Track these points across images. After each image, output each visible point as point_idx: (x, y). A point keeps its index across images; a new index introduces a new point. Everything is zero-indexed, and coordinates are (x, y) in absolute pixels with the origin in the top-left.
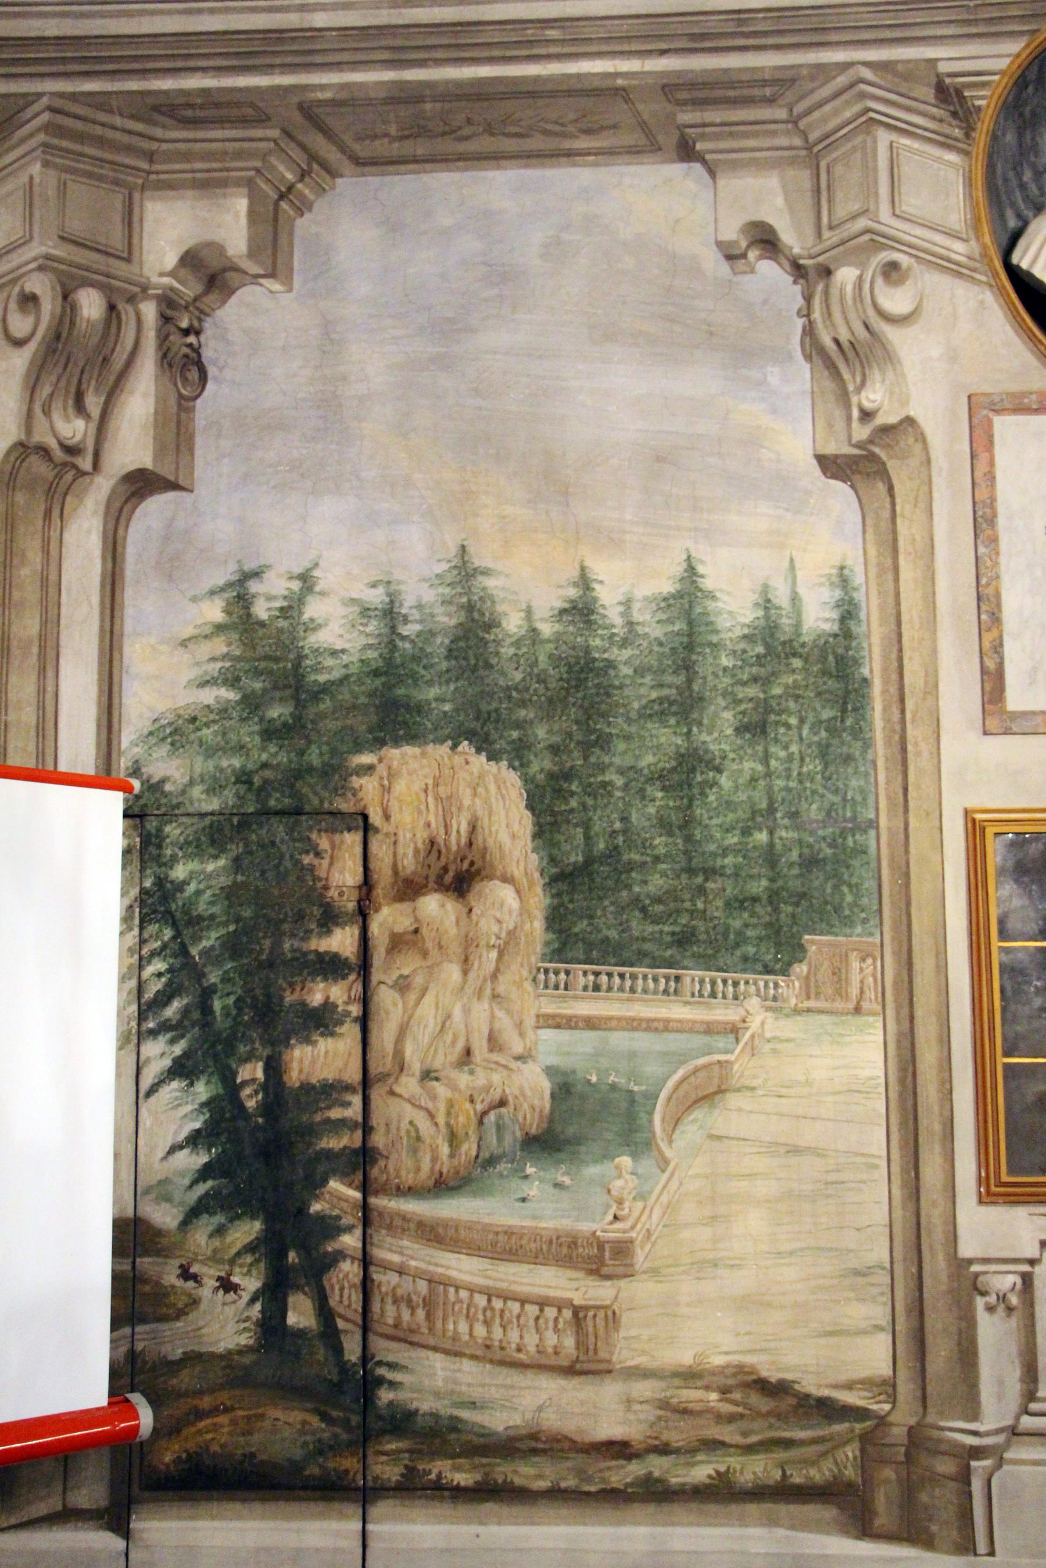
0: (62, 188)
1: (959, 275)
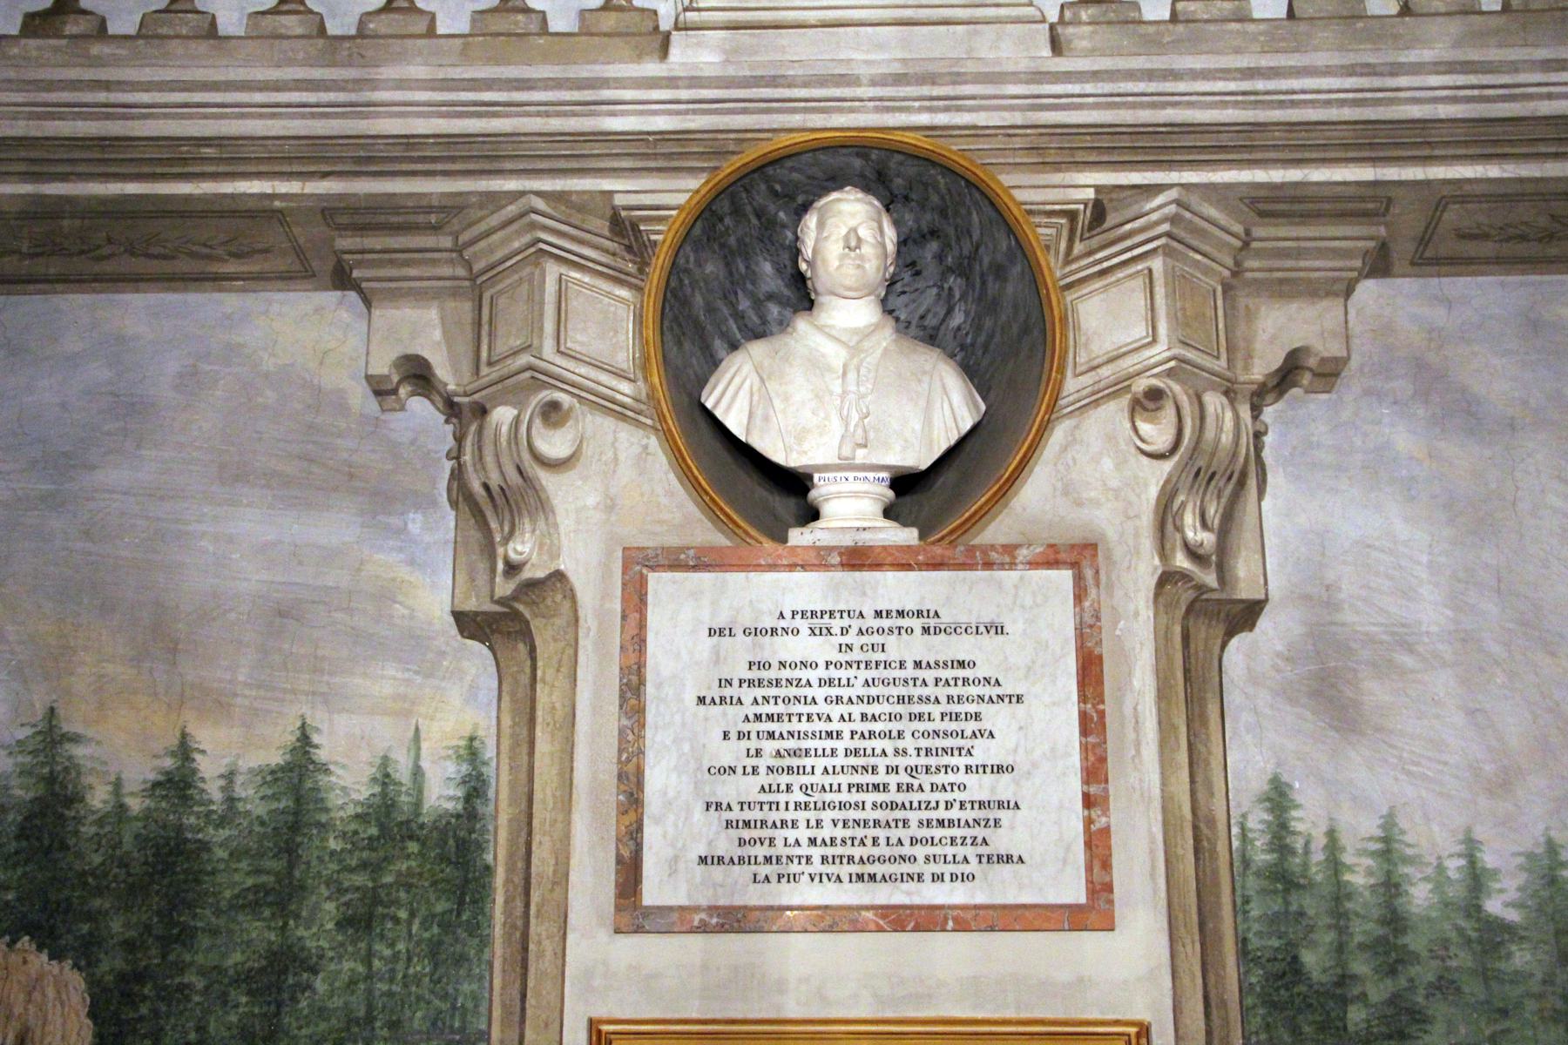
1: (622, 417)
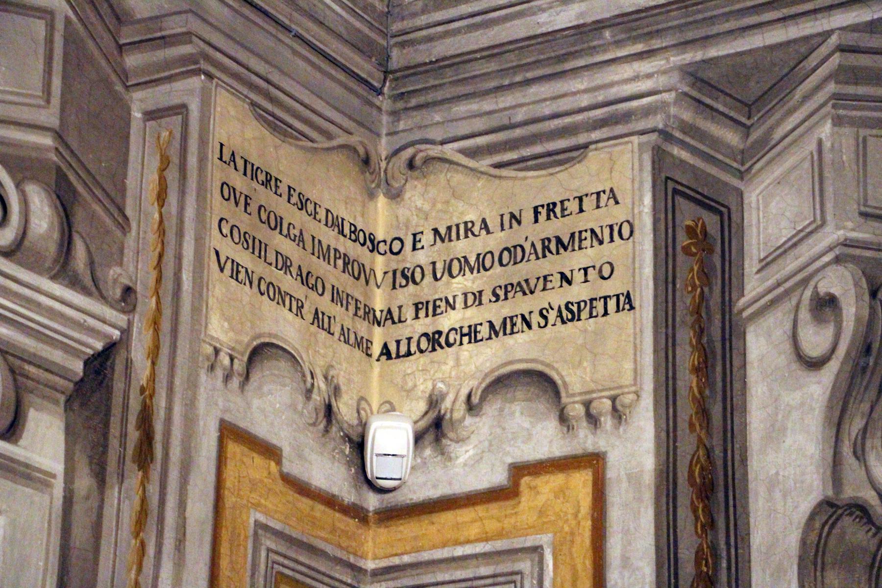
0: (862, 149)
